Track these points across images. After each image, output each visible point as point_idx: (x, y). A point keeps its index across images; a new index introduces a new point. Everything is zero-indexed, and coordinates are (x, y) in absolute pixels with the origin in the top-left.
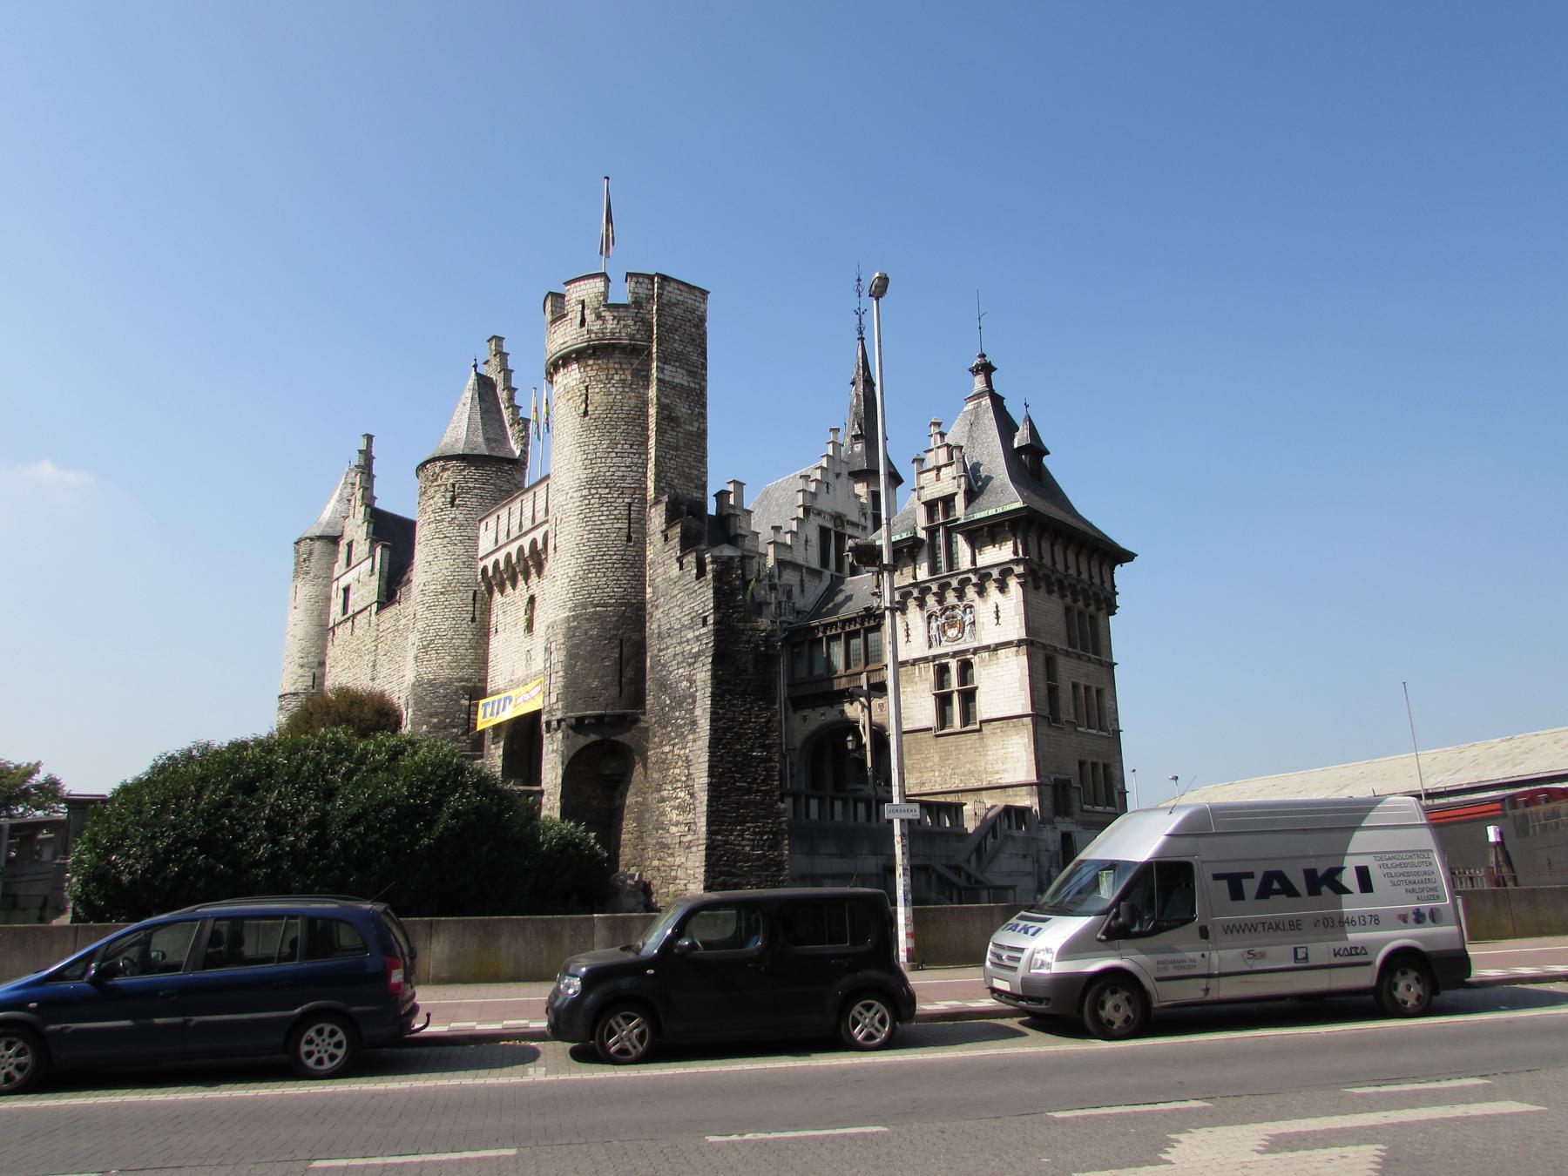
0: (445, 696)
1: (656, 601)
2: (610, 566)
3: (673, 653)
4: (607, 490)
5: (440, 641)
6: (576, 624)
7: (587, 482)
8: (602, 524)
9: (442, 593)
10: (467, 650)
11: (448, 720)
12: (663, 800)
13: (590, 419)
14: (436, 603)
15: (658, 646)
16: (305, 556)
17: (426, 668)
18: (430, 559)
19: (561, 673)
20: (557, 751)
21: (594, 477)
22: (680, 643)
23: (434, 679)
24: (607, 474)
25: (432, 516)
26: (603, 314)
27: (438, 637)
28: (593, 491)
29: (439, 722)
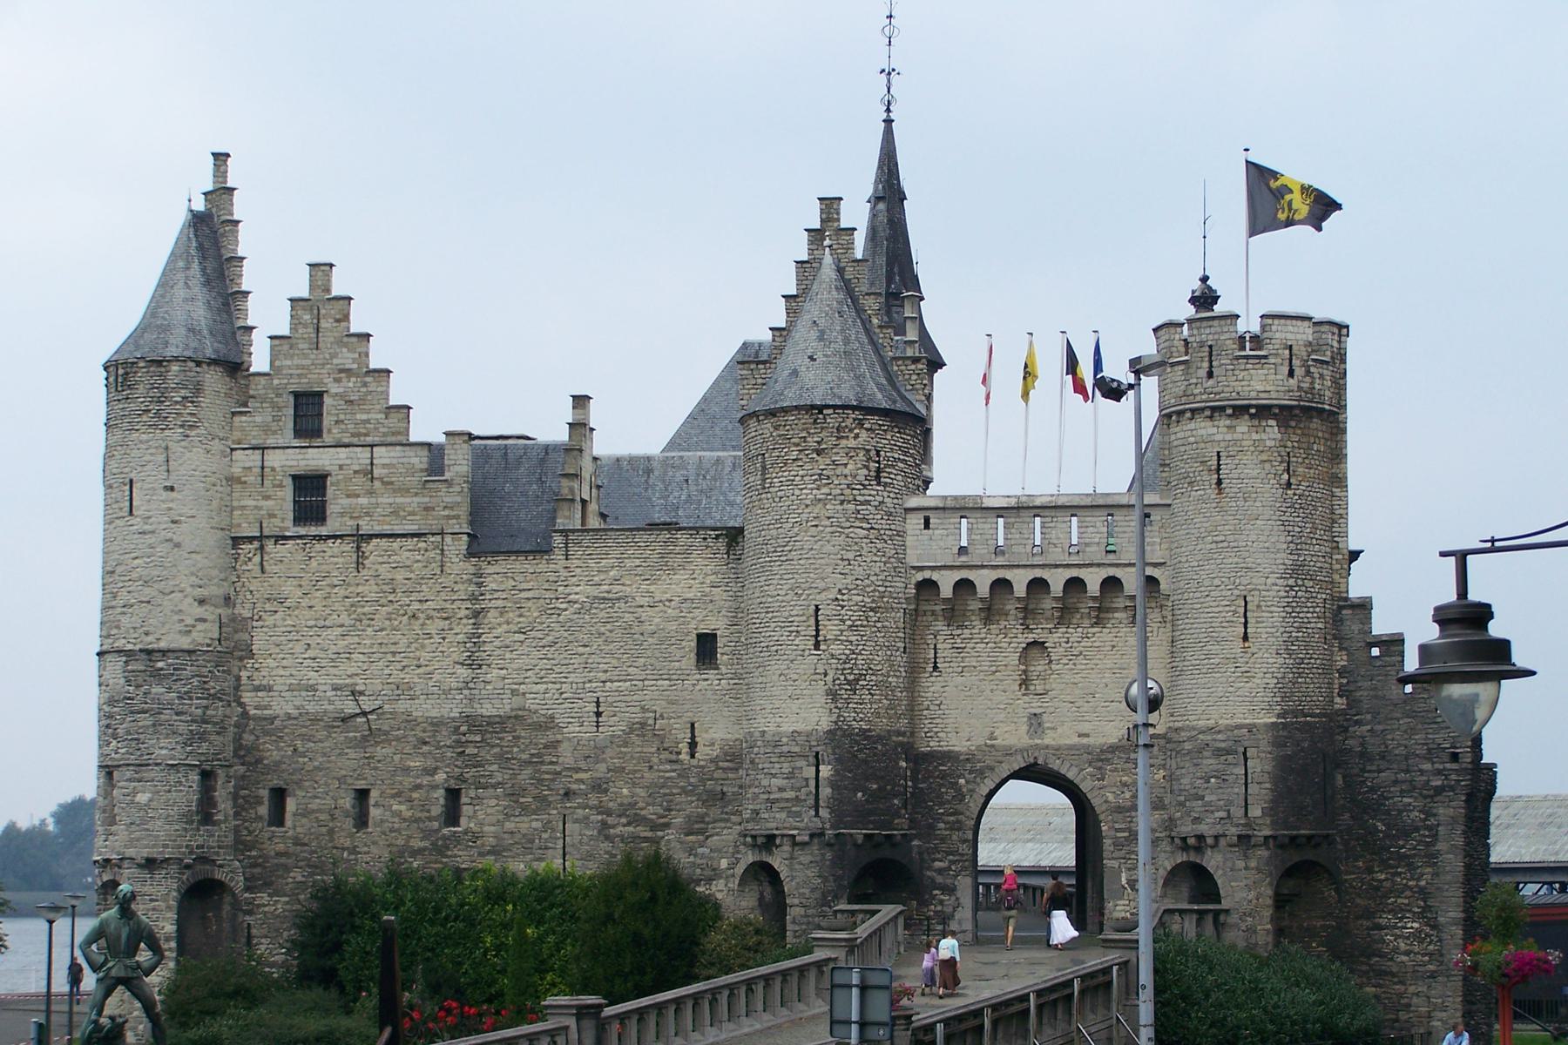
0: (884, 755)
1: (1355, 715)
2: (1315, 670)
3: (1393, 778)
4: (1311, 583)
5: (873, 678)
6: (1285, 734)
7: (1293, 570)
8: (1309, 622)
9: (872, 610)
10: (901, 692)
11: (889, 787)
12: (1380, 927)
13: (1295, 494)
14: (865, 623)
15: (1360, 766)
16: (183, 393)
17: (856, 712)
18: (850, 555)
19: (1268, 785)
20: (1257, 868)
21: (1300, 566)
22: (1407, 771)
23: (869, 730)
24: (1312, 563)
25: (848, 492)
26: (1312, 369)
27: (870, 672)
28: (1300, 582)
29: (879, 789)
